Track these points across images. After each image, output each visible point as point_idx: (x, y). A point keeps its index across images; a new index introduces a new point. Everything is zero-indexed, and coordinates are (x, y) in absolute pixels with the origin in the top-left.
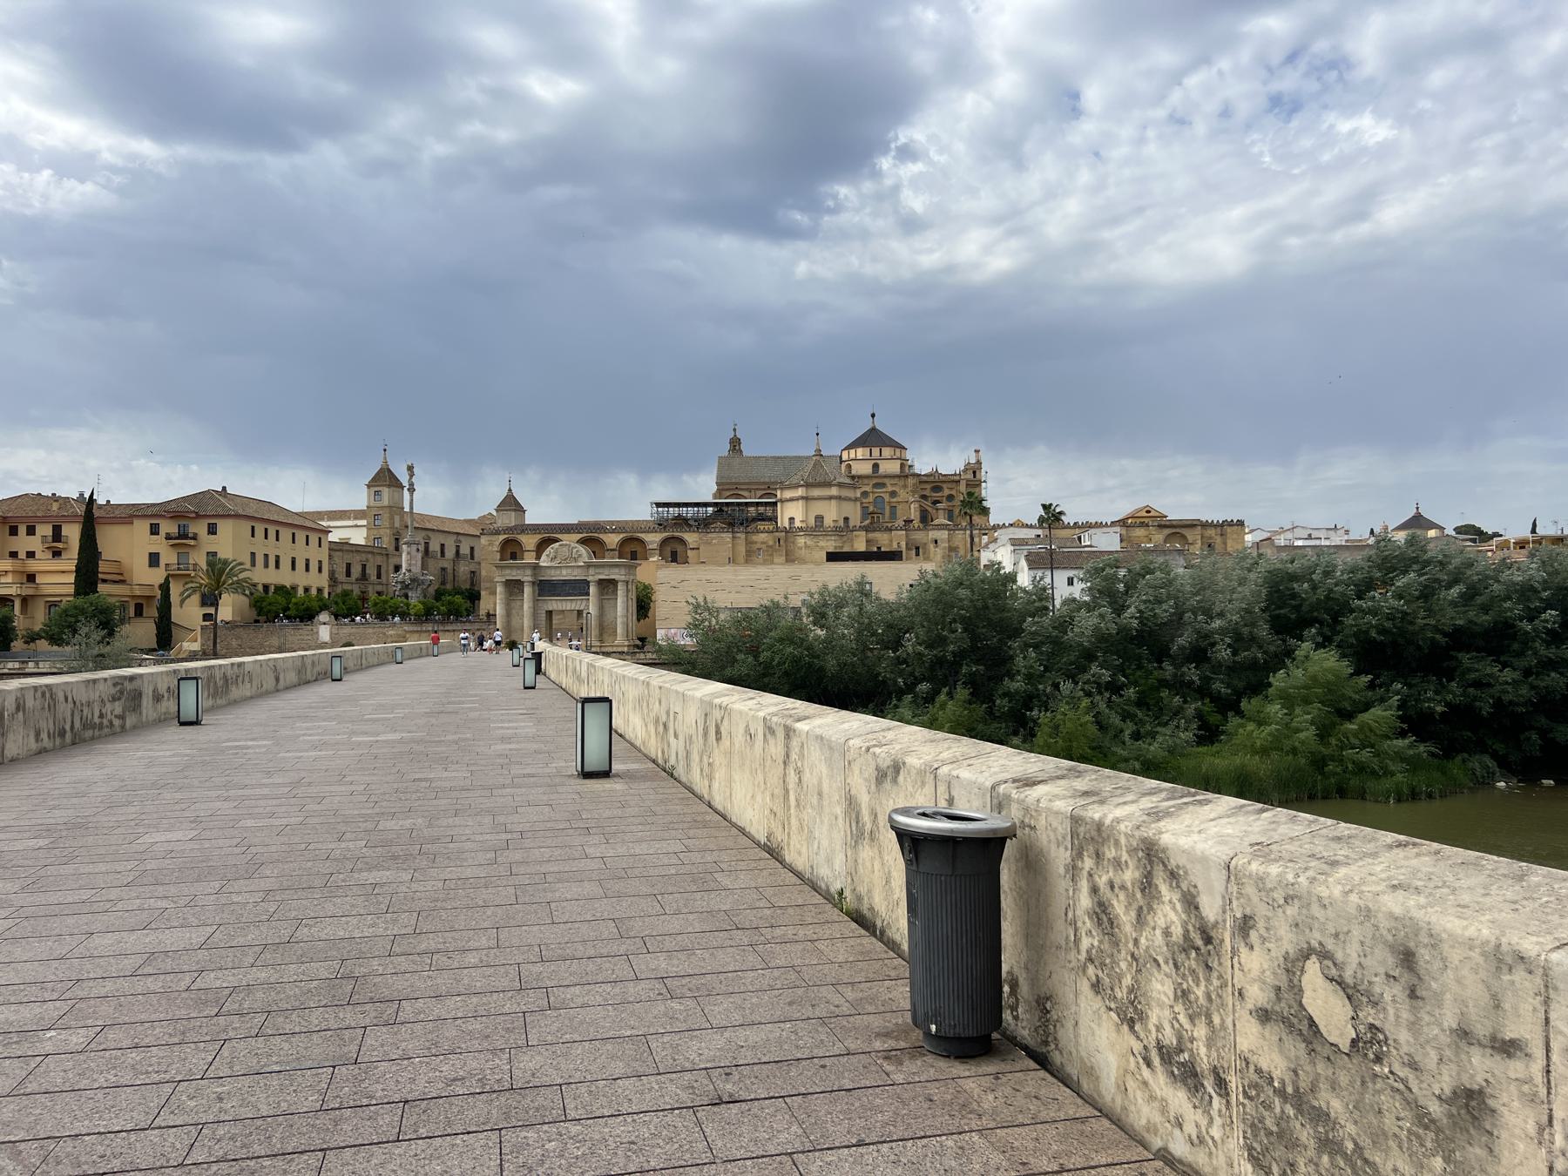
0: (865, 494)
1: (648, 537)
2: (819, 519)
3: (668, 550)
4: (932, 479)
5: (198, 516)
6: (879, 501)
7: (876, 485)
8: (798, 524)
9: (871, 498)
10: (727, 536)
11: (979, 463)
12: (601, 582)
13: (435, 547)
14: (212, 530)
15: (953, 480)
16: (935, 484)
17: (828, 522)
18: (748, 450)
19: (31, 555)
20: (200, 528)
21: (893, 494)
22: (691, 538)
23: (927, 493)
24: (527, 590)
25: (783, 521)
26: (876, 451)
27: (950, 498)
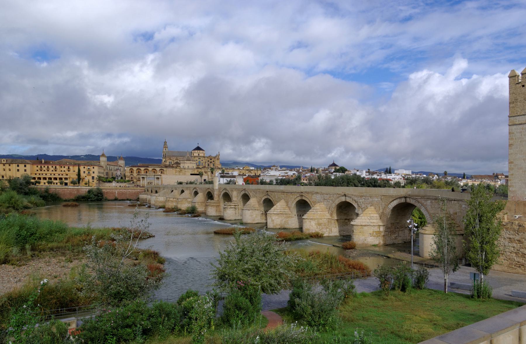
1: (157, 169)
2: (188, 166)
5: (92, 166)
7: (199, 159)
8: (184, 167)
9: (198, 161)
10: (172, 169)
11: (219, 154)
12: (157, 178)
13: (111, 168)
14: (93, 168)
16: (210, 157)
17: (190, 167)
19: (64, 171)
20: (92, 167)
22: (165, 169)
23: (209, 160)
24: (145, 179)
25: (182, 167)
26: (199, 151)
27: (214, 161)
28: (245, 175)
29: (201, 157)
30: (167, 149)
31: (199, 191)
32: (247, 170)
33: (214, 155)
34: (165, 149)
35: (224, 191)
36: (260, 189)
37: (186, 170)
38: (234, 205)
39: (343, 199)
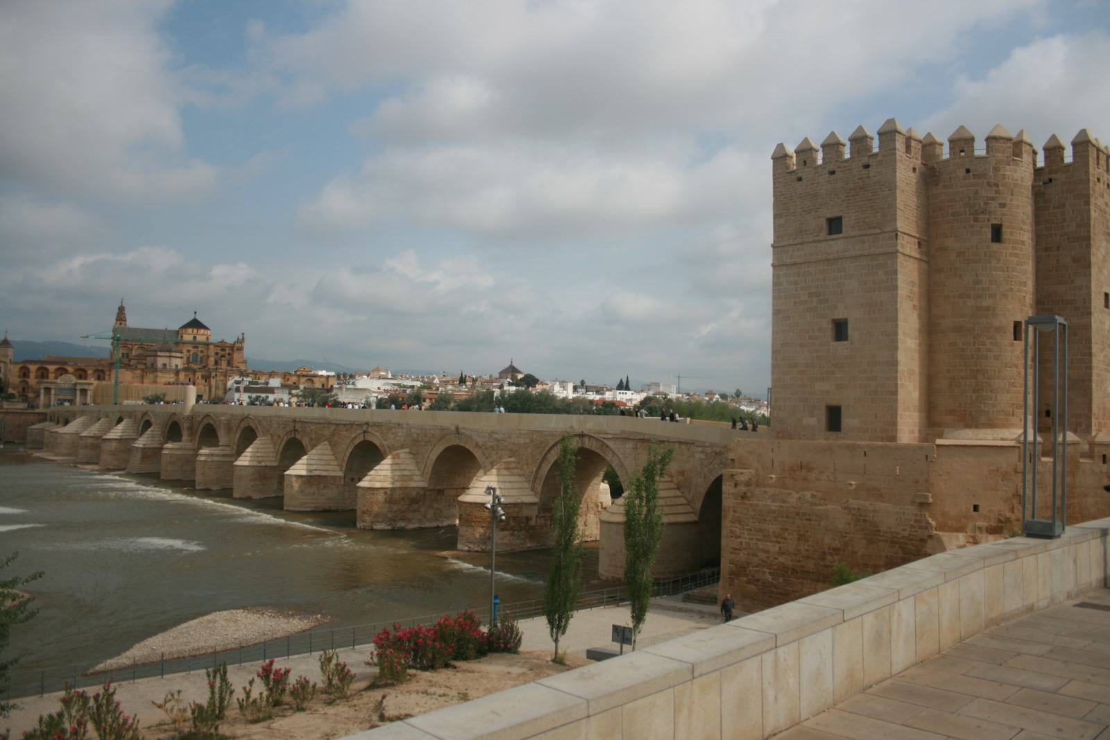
0: (188, 351)
3: (96, 375)
4: (220, 344)
6: (196, 355)
7: (194, 347)
9: (192, 352)
11: (243, 339)
15: (232, 347)
16: (222, 346)
17: (168, 367)
18: (132, 322)
21: (202, 352)
23: (219, 351)
24: (53, 392)
26: (195, 330)
27: (229, 354)
28: (297, 388)
29: (200, 343)
30: (123, 323)
31: (153, 420)
32: (304, 376)
33: (230, 340)
34: (118, 323)
35: (206, 421)
36: (279, 417)
37: (159, 374)
38: (223, 456)
39: (456, 442)
